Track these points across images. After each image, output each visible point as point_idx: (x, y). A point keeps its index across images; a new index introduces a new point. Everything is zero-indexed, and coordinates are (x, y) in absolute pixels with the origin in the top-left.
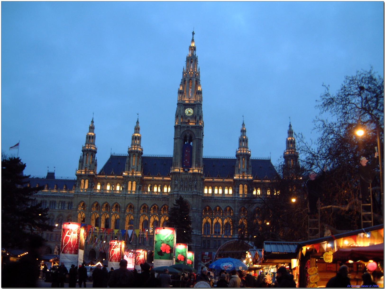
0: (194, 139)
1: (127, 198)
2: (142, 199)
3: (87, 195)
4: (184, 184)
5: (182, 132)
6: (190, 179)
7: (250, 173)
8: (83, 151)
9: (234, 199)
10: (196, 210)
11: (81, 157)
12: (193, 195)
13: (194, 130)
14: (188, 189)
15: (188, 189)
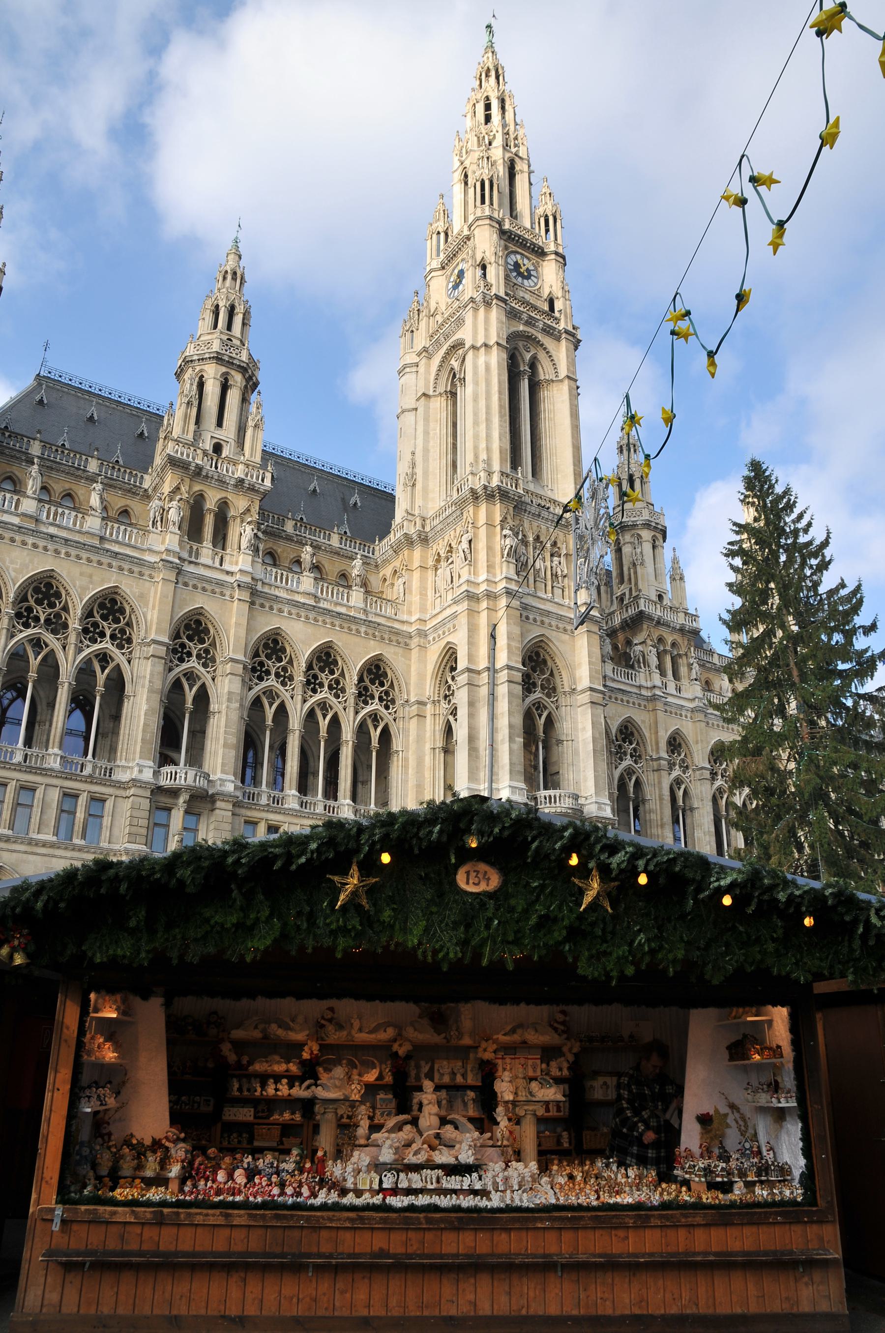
2: (267, 605)
14: (549, 588)
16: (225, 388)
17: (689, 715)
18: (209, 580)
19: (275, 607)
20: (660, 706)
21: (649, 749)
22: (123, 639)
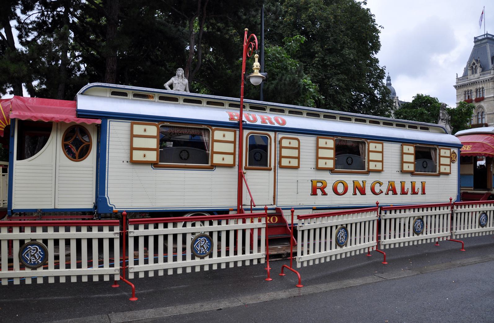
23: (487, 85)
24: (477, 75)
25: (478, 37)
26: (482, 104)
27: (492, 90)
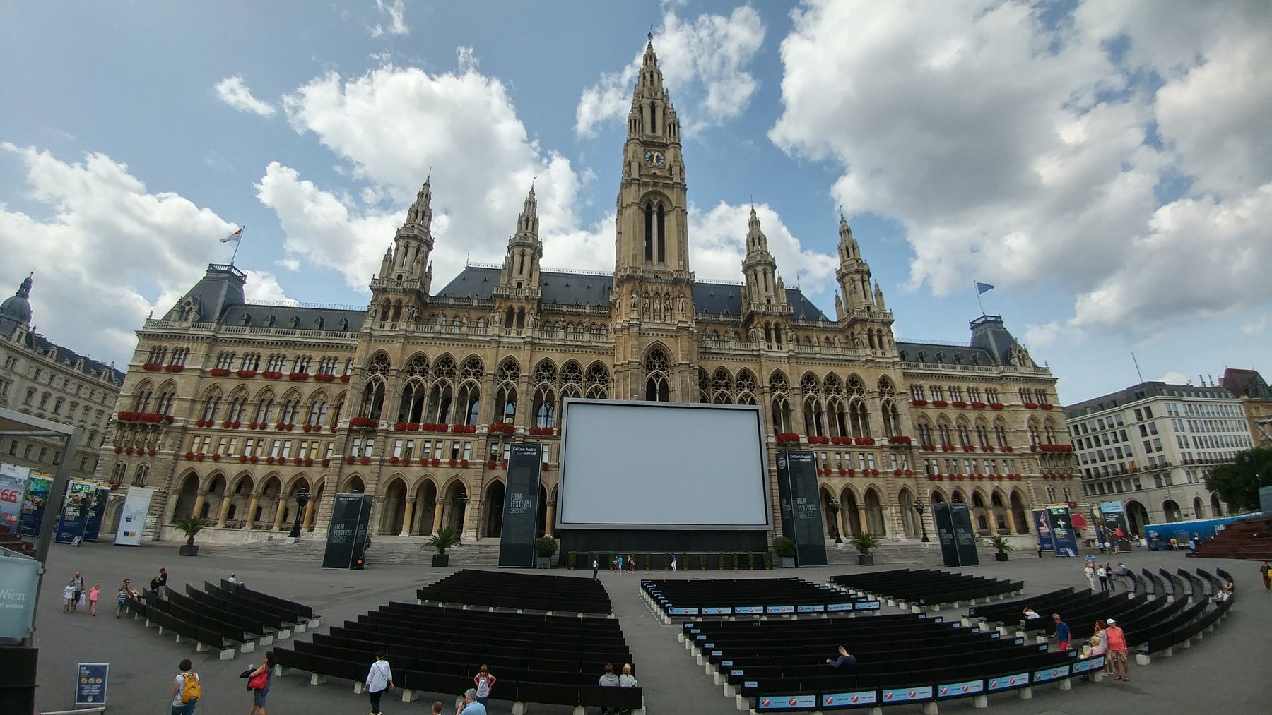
0: (669, 211)
1: (501, 345)
2: (542, 348)
3: (397, 336)
4: (652, 304)
5: (641, 194)
6: (667, 294)
7: (783, 298)
8: (396, 240)
9: (755, 353)
10: (689, 364)
11: (390, 250)
12: (679, 329)
13: (667, 192)
14: (663, 316)
15: (663, 316)
16: (523, 256)
17: (786, 361)
18: (513, 343)
19: (545, 349)
20: (763, 359)
21: (759, 382)
22: (478, 375)
23: (202, 346)
24: (185, 325)
25: (216, 265)
26: (176, 378)
27: (202, 357)
